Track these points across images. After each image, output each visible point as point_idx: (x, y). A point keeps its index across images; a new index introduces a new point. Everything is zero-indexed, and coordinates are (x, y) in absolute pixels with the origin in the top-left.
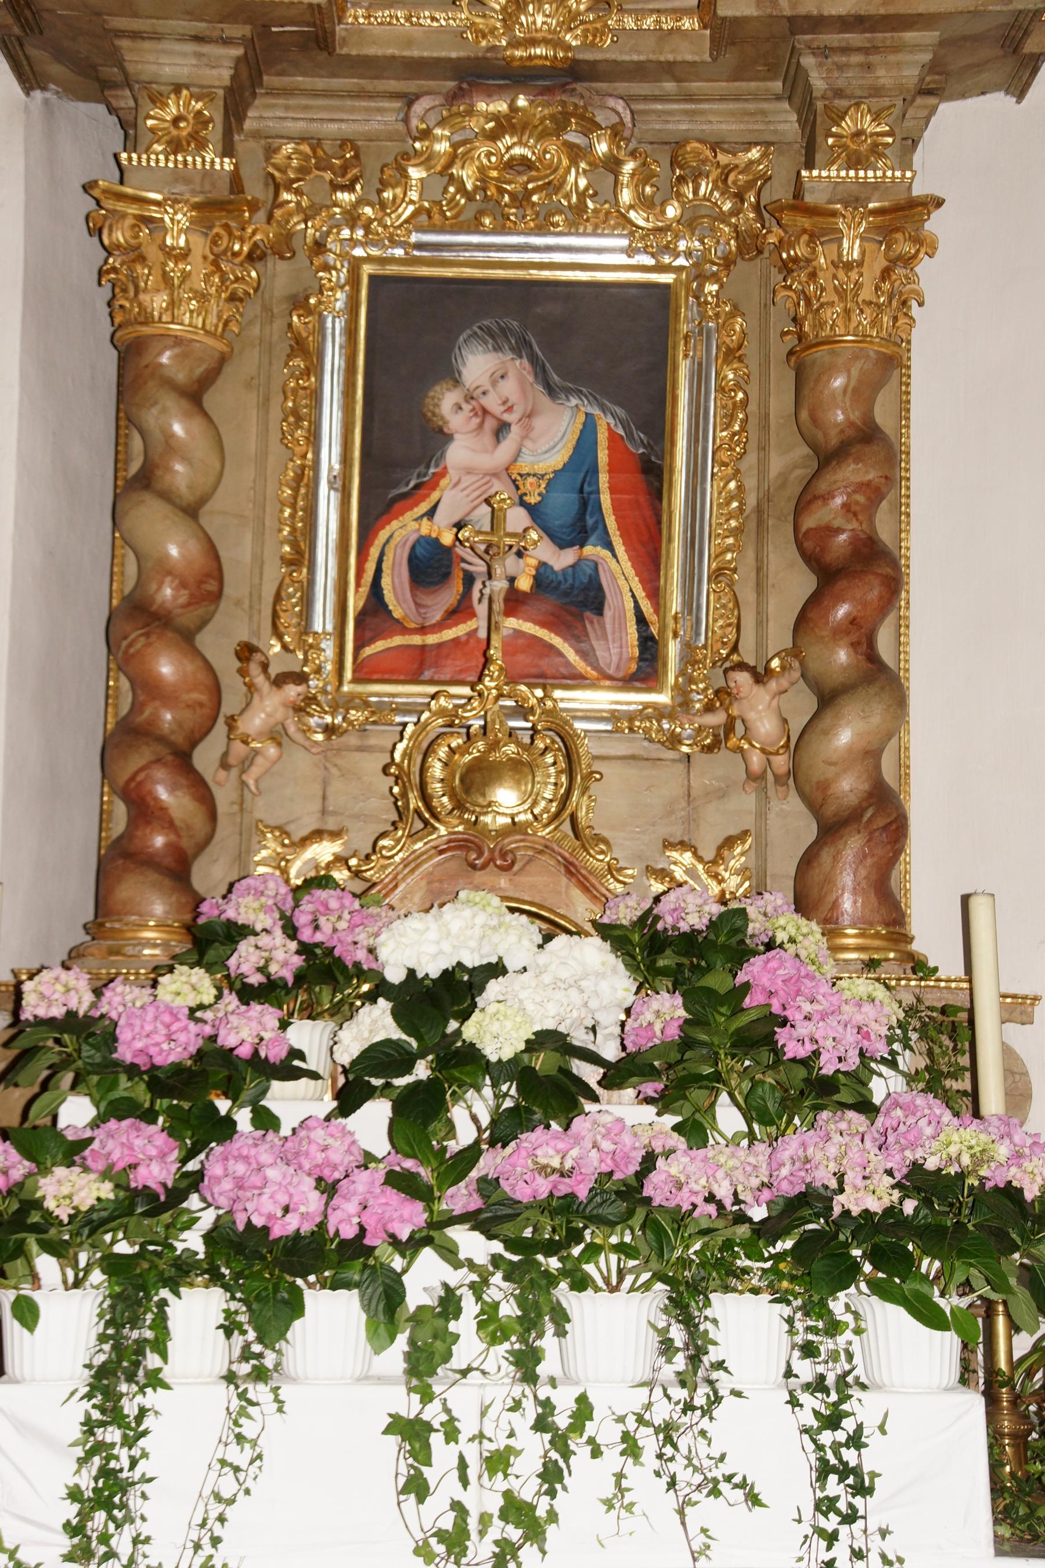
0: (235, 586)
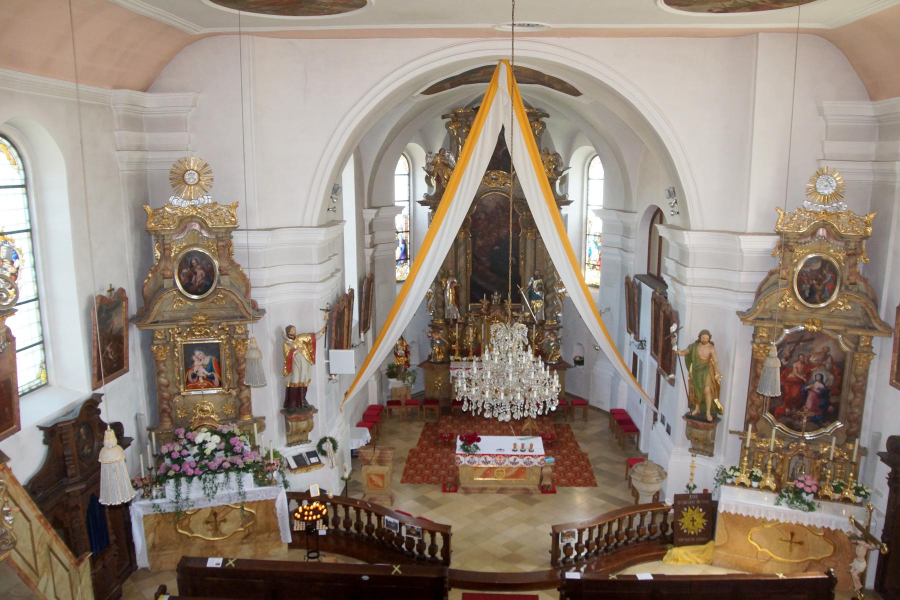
0: (171, 380)
